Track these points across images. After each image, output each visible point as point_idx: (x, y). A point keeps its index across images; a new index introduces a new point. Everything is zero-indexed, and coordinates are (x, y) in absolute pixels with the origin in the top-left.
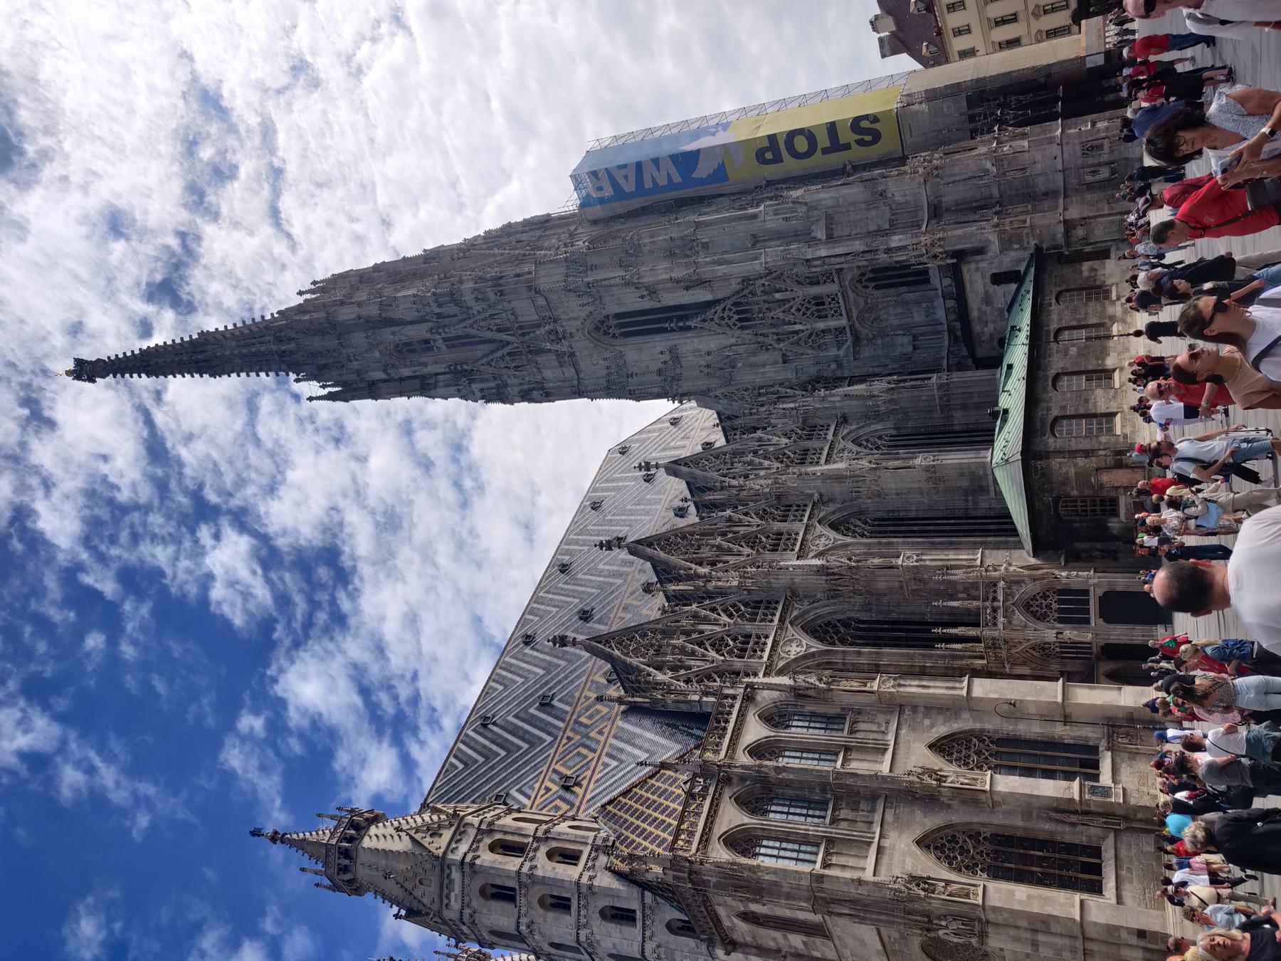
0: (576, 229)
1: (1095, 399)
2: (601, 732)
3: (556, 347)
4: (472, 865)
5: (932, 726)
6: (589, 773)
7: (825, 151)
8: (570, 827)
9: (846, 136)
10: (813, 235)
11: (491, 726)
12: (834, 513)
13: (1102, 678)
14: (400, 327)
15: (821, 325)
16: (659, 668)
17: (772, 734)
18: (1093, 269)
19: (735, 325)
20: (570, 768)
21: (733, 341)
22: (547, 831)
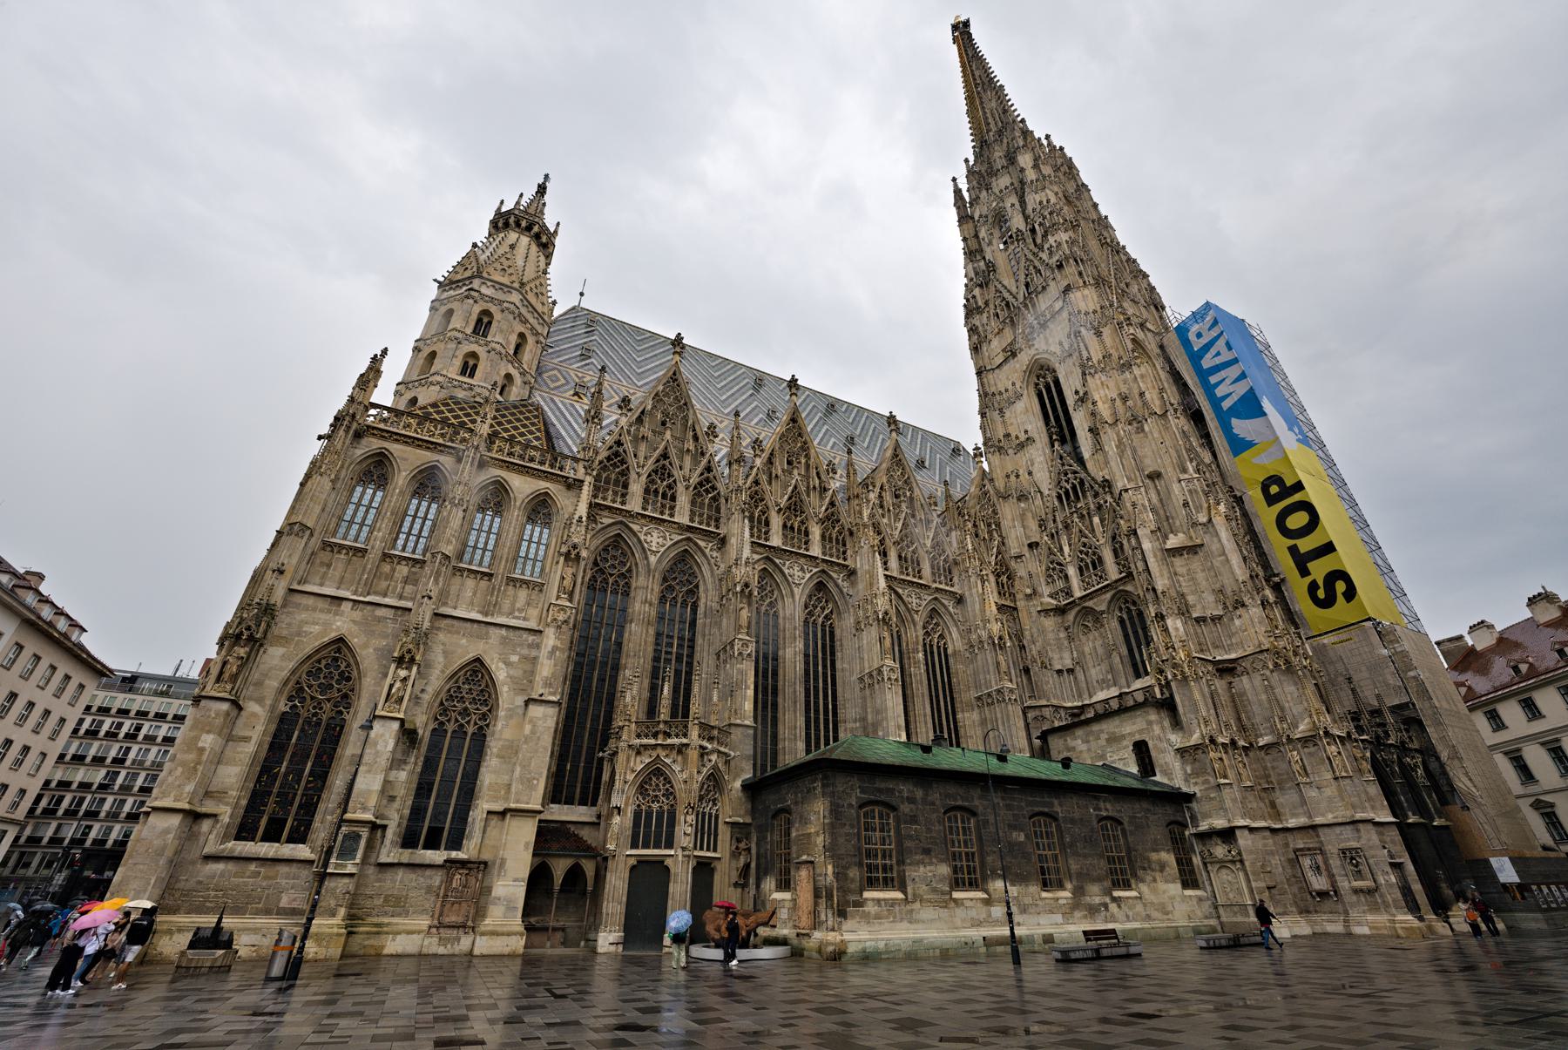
0: (1149, 330)
1: (931, 864)
4: (467, 297)
5: (508, 664)
7: (1293, 550)
8: (508, 377)
9: (1319, 569)
10: (1171, 536)
12: (837, 585)
15: (1072, 571)
17: (518, 504)
18: (1162, 867)
21: (1046, 492)
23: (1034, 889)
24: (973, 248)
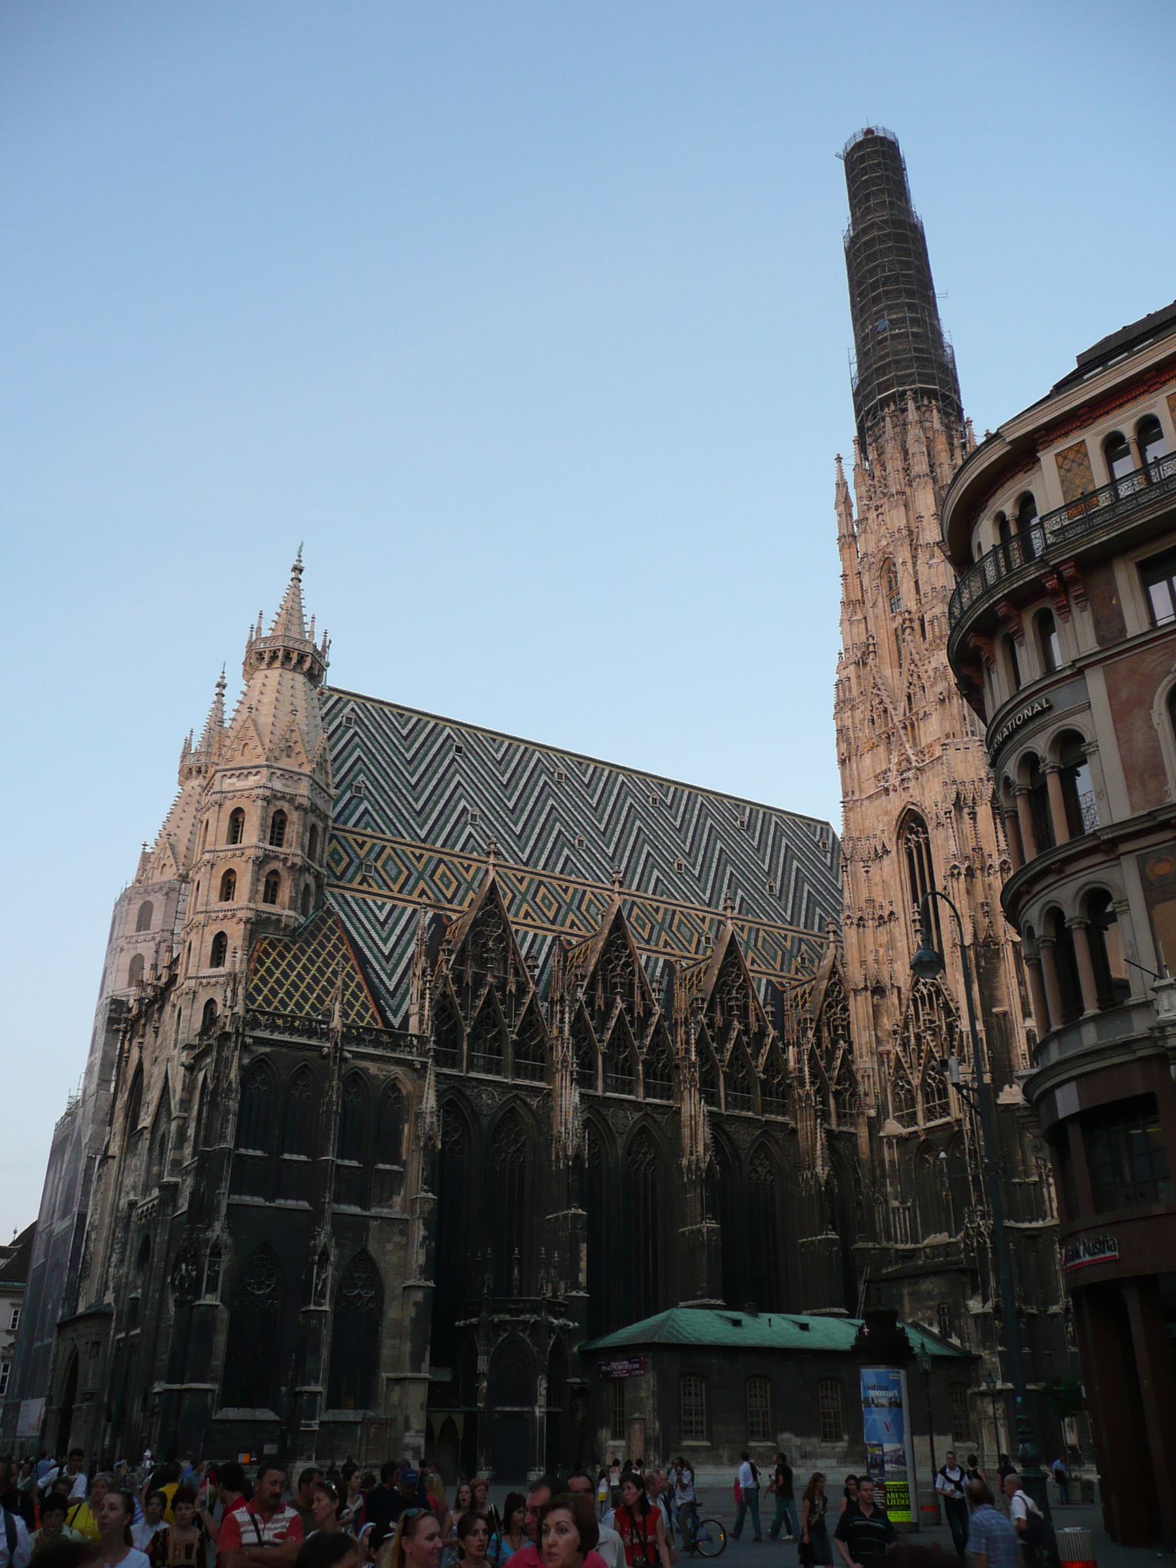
2: (423, 892)
3: (893, 767)
6: (375, 890)
8: (307, 886)
11: (450, 756)
13: (439, 1420)
14: (911, 571)
16: (460, 961)
19: (918, 991)
20: (383, 867)
22: (294, 865)
23: (815, 1441)
24: (853, 597)
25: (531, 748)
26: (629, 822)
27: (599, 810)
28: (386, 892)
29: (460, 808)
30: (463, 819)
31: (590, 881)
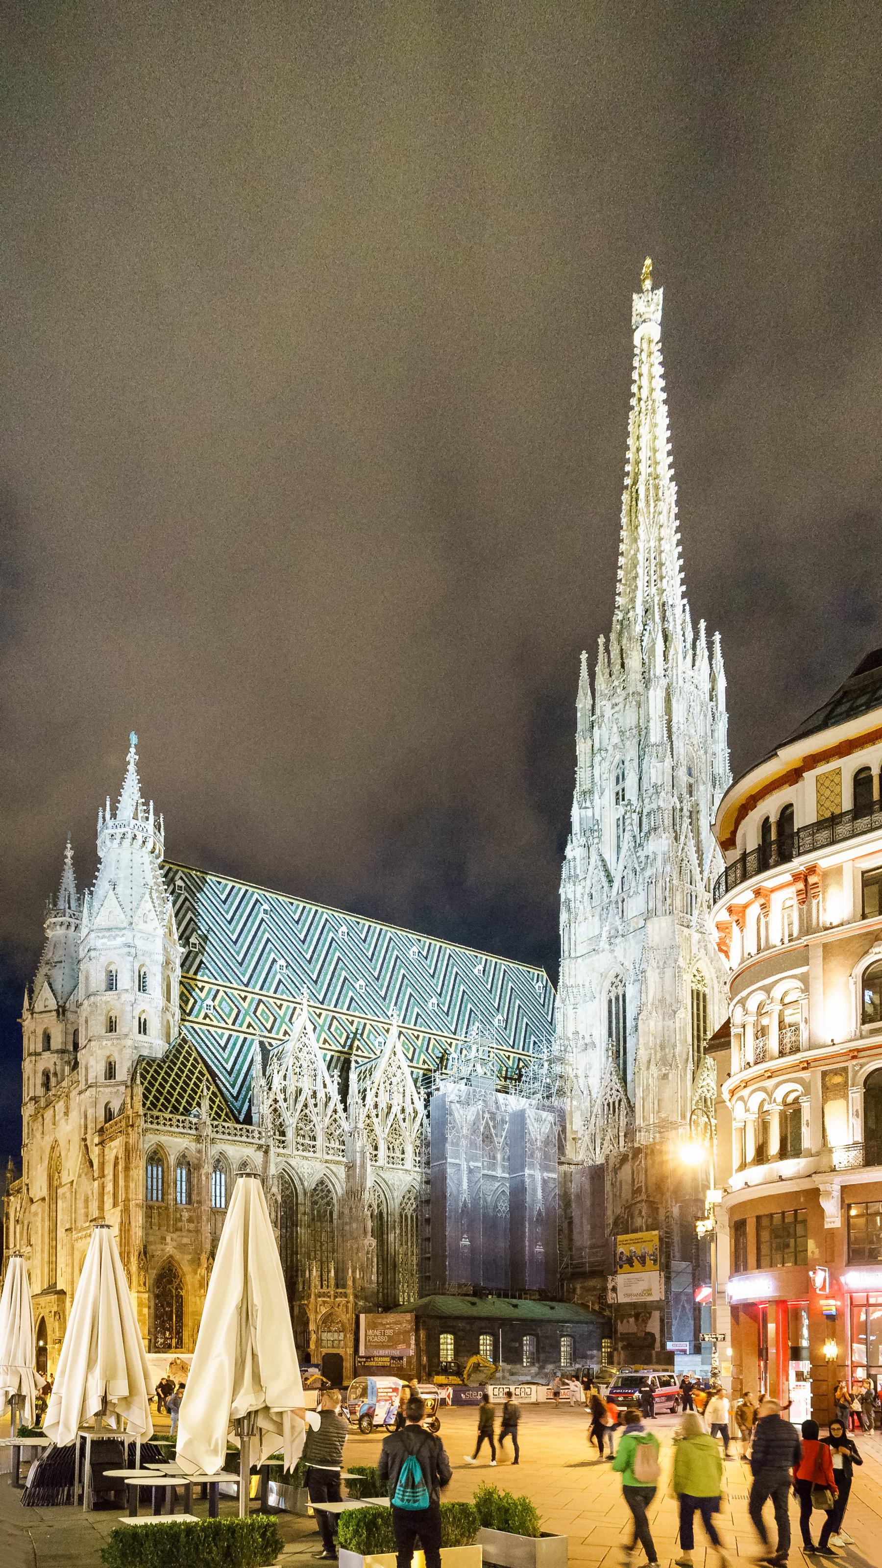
2: (249, 1025)
6: (215, 1023)
25: (320, 910)
26: (396, 971)
27: (374, 961)
28: (223, 1025)
29: (271, 959)
30: (273, 969)
31: (369, 1017)
